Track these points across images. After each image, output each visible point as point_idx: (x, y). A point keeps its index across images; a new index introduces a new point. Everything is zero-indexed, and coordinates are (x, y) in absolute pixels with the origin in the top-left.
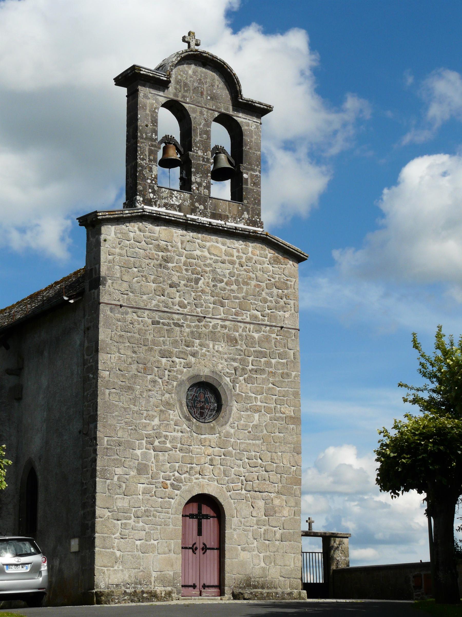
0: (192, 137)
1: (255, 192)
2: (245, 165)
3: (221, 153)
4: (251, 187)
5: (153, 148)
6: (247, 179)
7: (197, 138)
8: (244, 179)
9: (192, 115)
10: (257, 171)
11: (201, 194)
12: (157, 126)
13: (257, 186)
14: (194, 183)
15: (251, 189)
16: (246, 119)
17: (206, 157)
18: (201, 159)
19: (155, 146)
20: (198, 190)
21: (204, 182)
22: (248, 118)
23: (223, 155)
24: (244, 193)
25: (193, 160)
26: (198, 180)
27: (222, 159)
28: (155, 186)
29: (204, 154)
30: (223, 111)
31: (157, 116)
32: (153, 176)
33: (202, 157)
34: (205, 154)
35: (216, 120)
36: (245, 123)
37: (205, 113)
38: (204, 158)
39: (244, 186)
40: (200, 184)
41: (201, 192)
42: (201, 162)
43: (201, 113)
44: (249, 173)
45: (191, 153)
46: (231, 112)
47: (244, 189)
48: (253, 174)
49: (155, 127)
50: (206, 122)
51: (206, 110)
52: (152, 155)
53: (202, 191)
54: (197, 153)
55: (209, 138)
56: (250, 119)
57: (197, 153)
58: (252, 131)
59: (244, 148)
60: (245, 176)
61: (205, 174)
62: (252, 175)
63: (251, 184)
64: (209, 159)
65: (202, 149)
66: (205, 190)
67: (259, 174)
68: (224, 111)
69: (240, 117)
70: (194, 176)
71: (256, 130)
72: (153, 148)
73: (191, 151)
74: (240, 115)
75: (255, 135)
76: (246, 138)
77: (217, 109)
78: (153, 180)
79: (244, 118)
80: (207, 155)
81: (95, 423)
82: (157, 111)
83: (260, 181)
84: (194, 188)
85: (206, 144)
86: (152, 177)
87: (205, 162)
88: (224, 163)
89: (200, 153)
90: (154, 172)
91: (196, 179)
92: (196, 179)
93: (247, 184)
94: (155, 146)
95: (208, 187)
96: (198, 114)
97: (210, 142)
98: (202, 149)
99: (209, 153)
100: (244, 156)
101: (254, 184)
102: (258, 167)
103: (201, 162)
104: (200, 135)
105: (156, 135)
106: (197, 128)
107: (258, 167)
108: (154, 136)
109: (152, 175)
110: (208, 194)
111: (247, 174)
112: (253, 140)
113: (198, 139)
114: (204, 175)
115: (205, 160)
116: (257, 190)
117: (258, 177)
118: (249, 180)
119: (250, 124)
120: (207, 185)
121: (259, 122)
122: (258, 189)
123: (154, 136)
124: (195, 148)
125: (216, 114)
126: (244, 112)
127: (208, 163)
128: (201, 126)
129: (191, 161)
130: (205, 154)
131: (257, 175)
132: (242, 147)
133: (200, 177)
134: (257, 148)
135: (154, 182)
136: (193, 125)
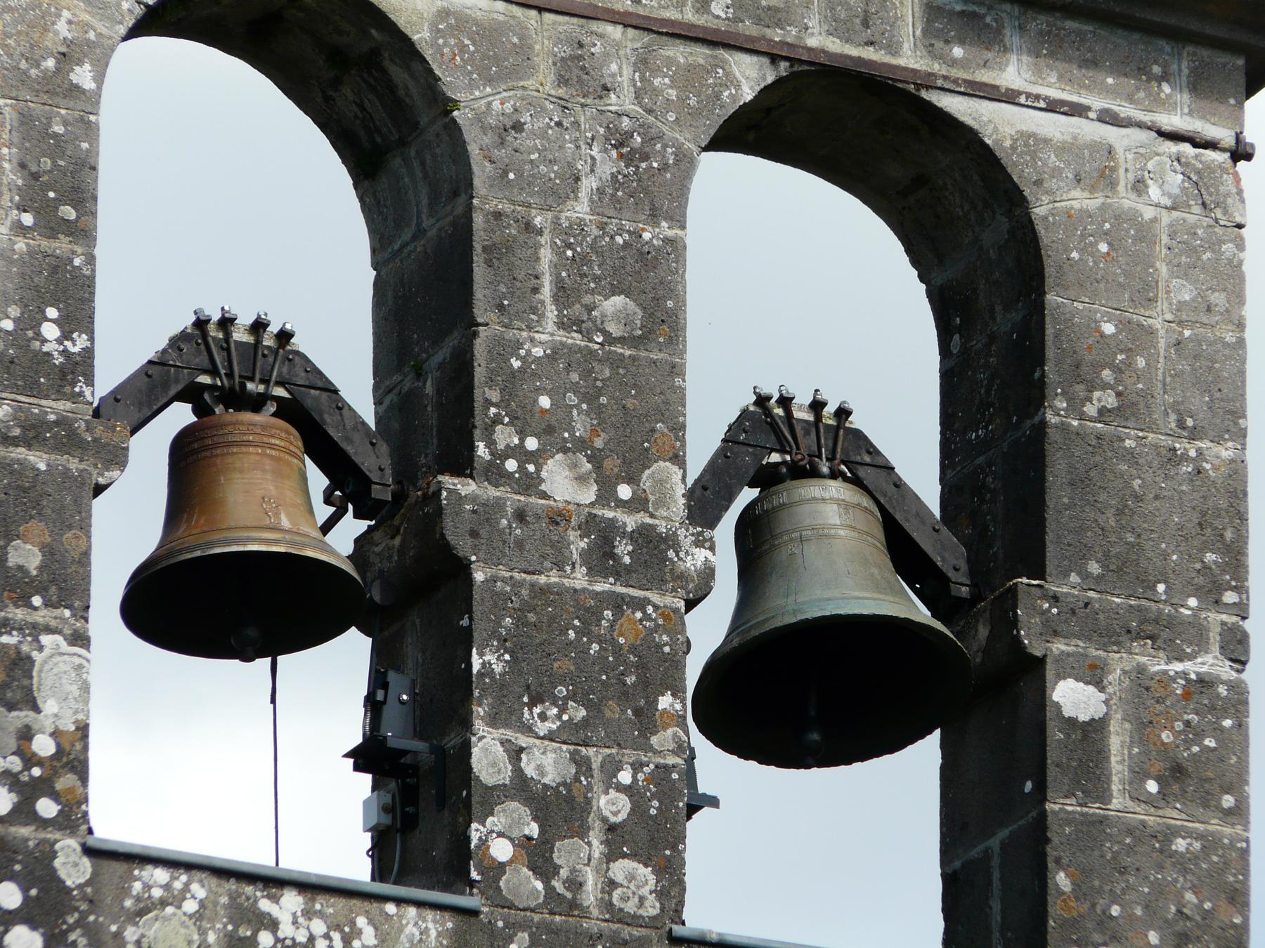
0: (470, 326)
1: (1183, 863)
2: (1068, 586)
3: (813, 473)
4: (1142, 815)
5: (39, 461)
6: (1093, 731)
7: (523, 335)
8: (1055, 735)
9: (477, 103)
10: (1202, 645)
11: (573, 907)
12: (83, 232)
13: (1208, 801)
14: (493, 797)
15: (1138, 832)
16: (1077, 110)
17: (631, 521)
18: (578, 544)
19: (63, 437)
20: (545, 869)
21: (610, 783)
22: (1096, 103)
23: (836, 489)
24: (1062, 880)
25: (492, 559)
26: (547, 764)
27: (822, 534)
28: (67, 847)
29: (606, 495)
30: (820, 39)
31: (90, 130)
32: (44, 746)
33: (590, 524)
34: (624, 492)
35: (745, 132)
36: (1063, 149)
37: (621, 72)
38: (604, 535)
39: (1061, 806)
40: (560, 811)
41: (575, 884)
42: (579, 579)
43: (578, 72)
44: (1119, 663)
45: (466, 487)
46: (910, 56)
47: (1058, 835)
48: (1165, 680)
49: (62, 245)
50: (628, 159)
51: (632, 40)
52: (35, 527)
53: (591, 881)
54: (530, 484)
55: (662, 322)
56: (1126, 110)
57: (535, 483)
58: (1145, 232)
59: (1057, 412)
60: (1072, 697)
61: (625, 695)
62: (1141, 682)
63: (1139, 775)
64: (670, 540)
65: (582, 445)
66: (621, 869)
67: (1225, 671)
68: (835, 46)
69: (1010, 97)
70: (493, 720)
71: (1194, 216)
72: (39, 461)
73: (463, 465)
74: (1013, 72)
75: (1182, 271)
76: (1080, 310)
77: (748, 28)
78: (44, 787)
79: (1053, 107)
80: (638, 503)
81: (949, 871)
82: (83, 76)
83: (1237, 741)
84: (501, 850)
85: (631, 398)
86: (30, 760)
87: (620, 573)
88: (842, 573)
89: (563, 483)
90: (50, 706)
91: (516, 754)
92: (516, 754)
93: (1091, 778)
94: (63, 437)
95: (658, 831)
96: (543, 80)
97: (676, 370)
98: (582, 445)
99: (661, 482)
100: (1058, 494)
101: (1176, 774)
102: (1211, 595)
103: (579, 579)
104: (563, 294)
105: (79, 318)
106: (528, 227)
107: (1211, 595)
108: (50, 331)
109: (26, 735)
110: (652, 908)
111: (1094, 675)
112: (1158, 319)
113: (545, 335)
114: (612, 710)
115: (624, 550)
116: (1210, 843)
117: (1218, 708)
118: (1117, 742)
119: (1125, 158)
120: (638, 809)
121: (1225, 136)
122: (1215, 826)
123: (50, 331)
124: (505, 436)
125: (747, 78)
126: (1049, 48)
127: (658, 583)
128: (580, 209)
129: (464, 569)
130: (624, 492)
131: (1205, 683)
132: (1035, 395)
133: (572, 735)
134: (1198, 402)
135: (47, 808)
136: (486, 197)
